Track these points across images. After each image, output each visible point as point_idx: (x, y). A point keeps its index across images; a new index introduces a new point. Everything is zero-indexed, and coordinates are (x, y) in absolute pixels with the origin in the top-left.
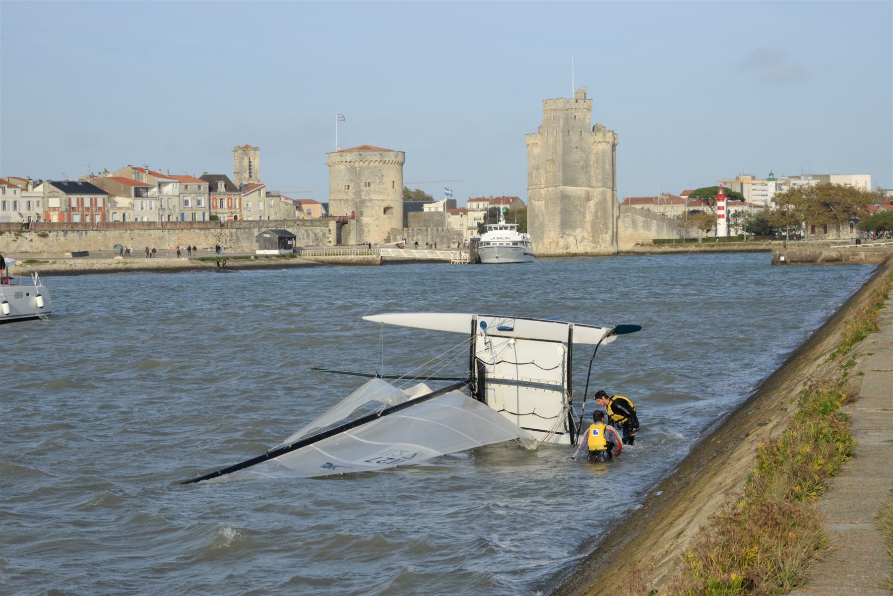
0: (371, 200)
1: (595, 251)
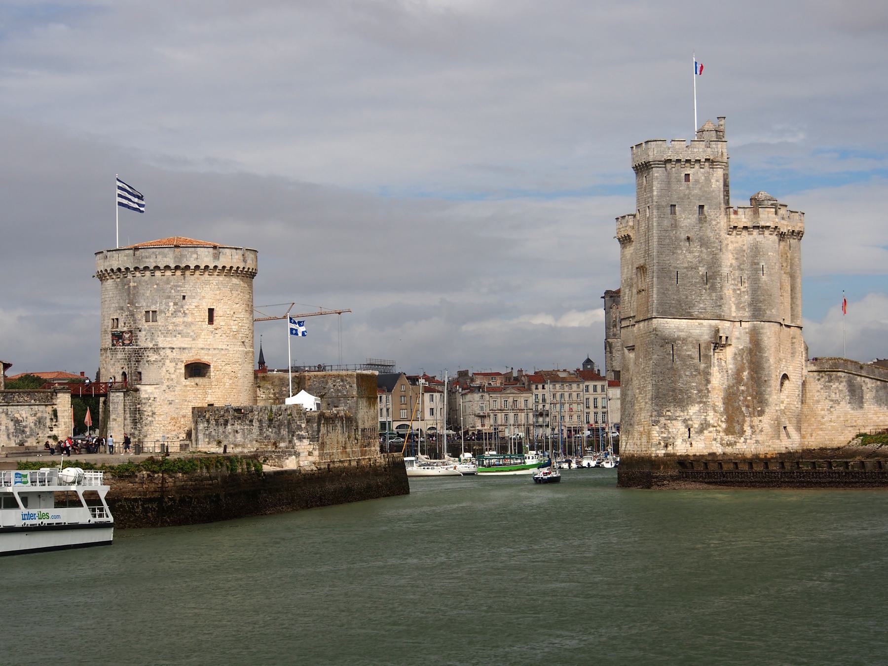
0: (156, 349)
1: (729, 450)
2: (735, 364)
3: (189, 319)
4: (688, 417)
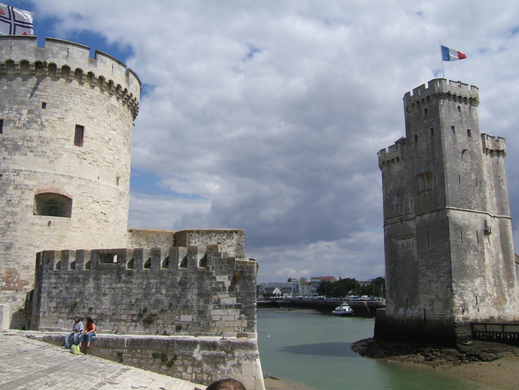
1: (501, 313)
2: (495, 248)
3: (47, 134)
4: (474, 288)
